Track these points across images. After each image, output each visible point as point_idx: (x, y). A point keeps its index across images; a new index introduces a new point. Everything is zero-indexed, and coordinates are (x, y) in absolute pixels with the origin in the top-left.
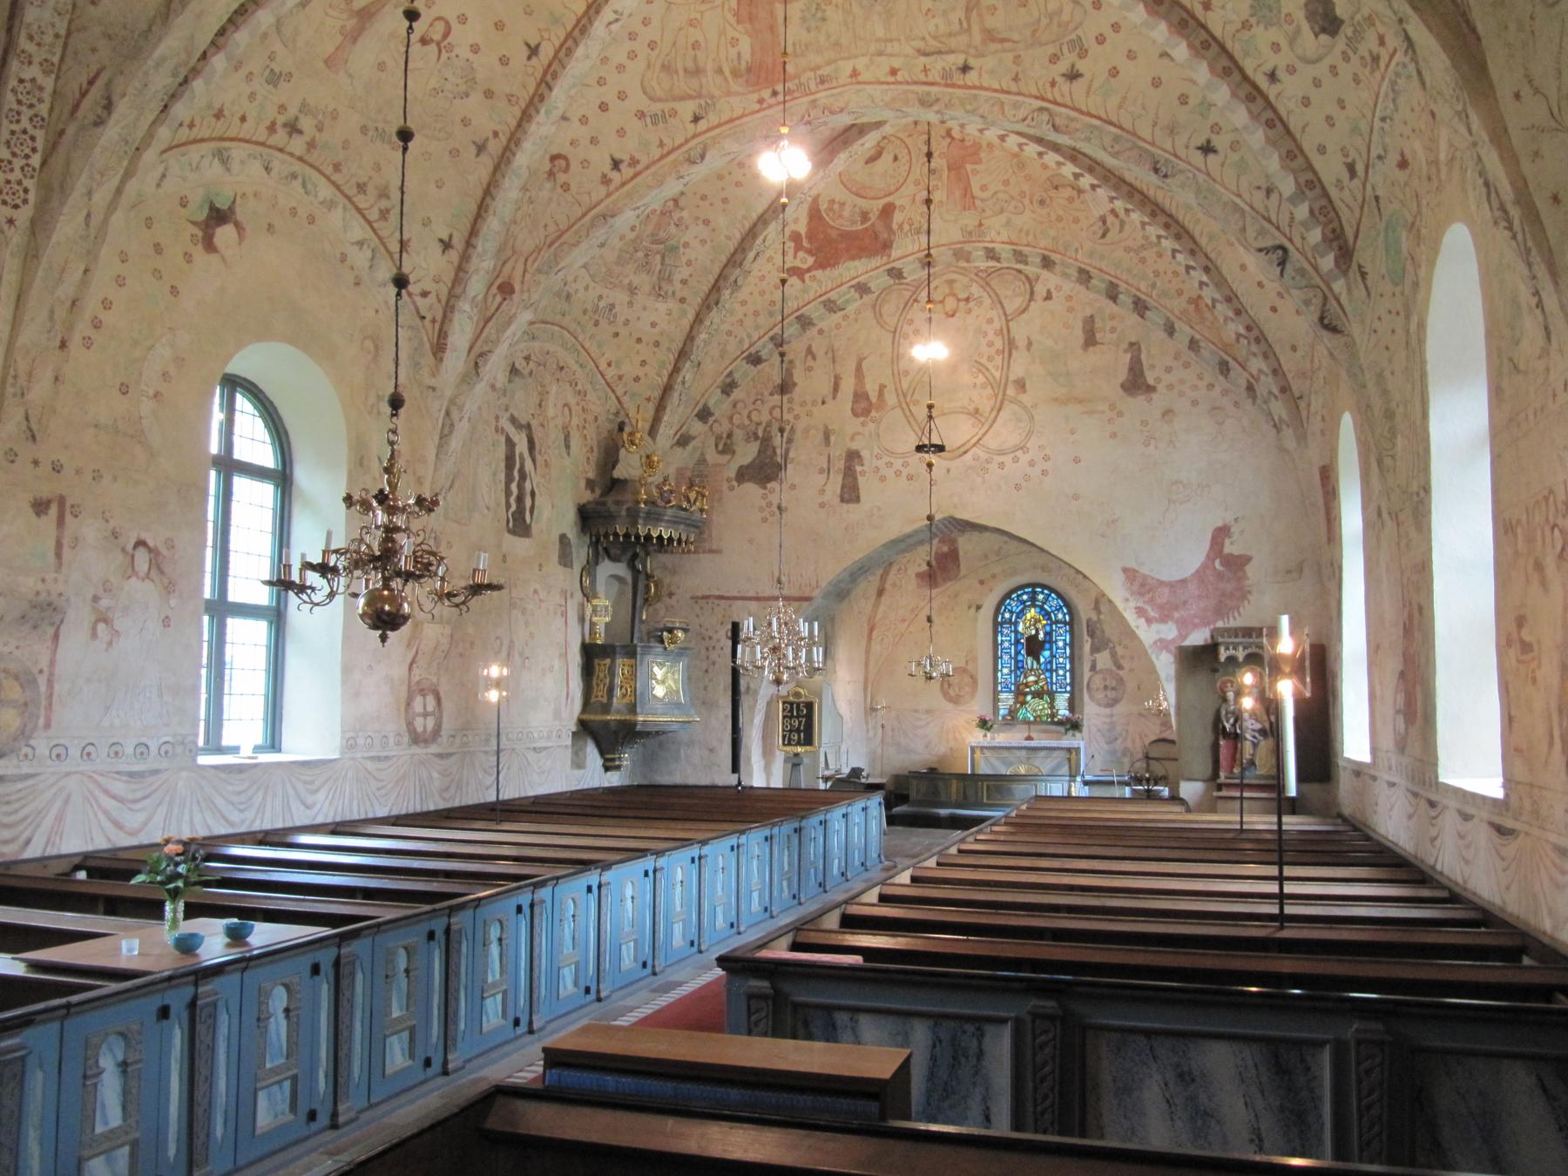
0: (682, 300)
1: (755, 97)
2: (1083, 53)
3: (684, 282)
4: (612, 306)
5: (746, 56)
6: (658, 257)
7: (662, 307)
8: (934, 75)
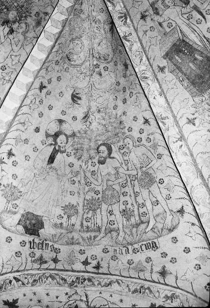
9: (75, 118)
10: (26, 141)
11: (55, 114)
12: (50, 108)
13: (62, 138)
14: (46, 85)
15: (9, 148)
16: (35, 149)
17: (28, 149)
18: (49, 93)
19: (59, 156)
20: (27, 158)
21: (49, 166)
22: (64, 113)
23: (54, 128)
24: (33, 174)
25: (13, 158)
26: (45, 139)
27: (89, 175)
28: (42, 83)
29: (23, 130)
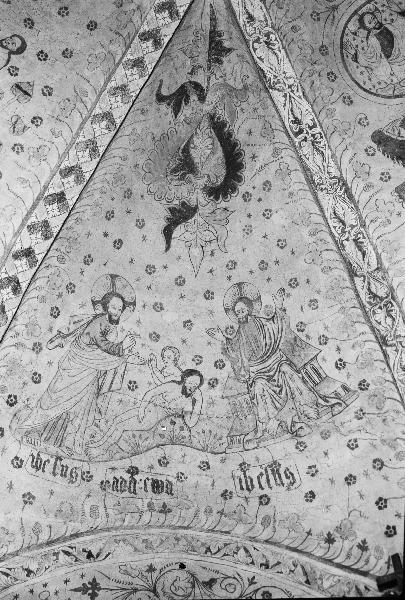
0: (363, 386)
3: (340, 365)
4: (274, 467)
6: (285, 368)
7: (347, 416)
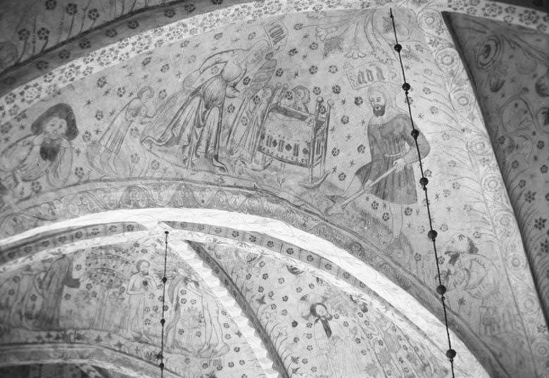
1: (37, 334)
2: (220, 368)
5: (38, 308)
8: (142, 354)
9: (311, 286)
10: (296, 340)
11: (294, 298)
12: (285, 299)
13: (319, 309)
14: (262, 294)
15: (289, 358)
16: (309, 336)
17: (303, 342)
18: (271, 295)
19: (331, 324)
20: (309, 348)
21: (331, 338)
22: (299, 290)
23: (305, 308)
24: (325, 356)
25: (300, 360)
26: (307, 322)
27: (364, 326)
28: (257, 300)
29: (284, 337)
